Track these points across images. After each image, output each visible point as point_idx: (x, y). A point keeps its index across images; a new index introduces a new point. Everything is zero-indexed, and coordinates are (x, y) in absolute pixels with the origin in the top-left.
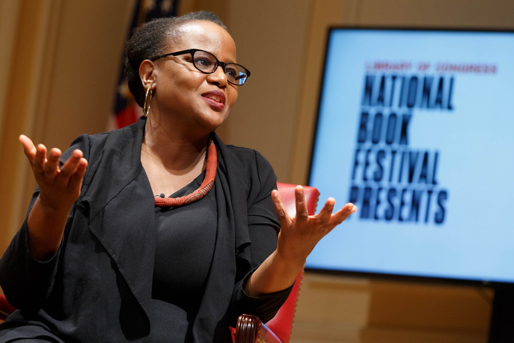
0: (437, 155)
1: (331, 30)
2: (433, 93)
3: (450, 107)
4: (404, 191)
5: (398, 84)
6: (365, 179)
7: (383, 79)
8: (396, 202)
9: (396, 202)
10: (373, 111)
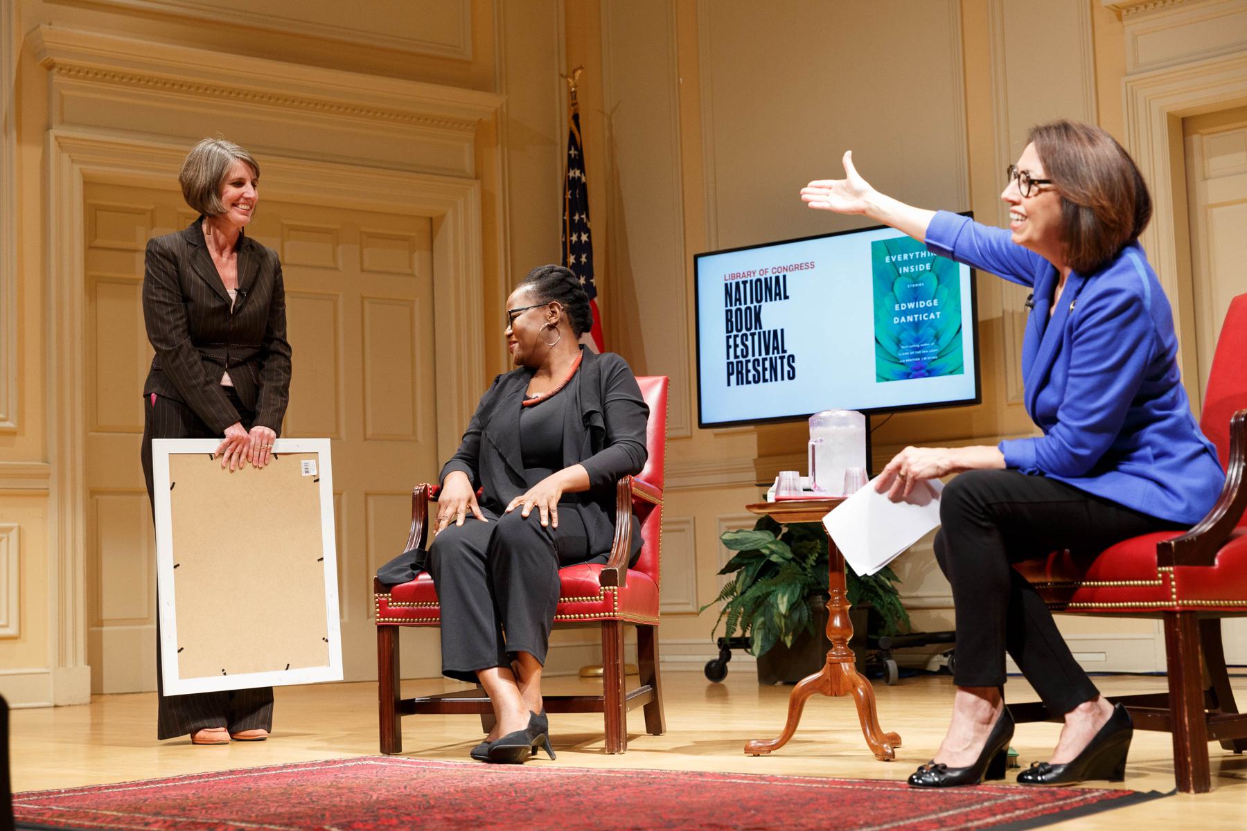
0: (782, 331)
1: (696, 257)
2: (774, 289)
3: (786, 297)
4: (764, 360)
5: (748, 285)
6: (736, 357)
7: (737, 284)
8: (760, 369)
9: (760, 369)
10: (734, 308)
